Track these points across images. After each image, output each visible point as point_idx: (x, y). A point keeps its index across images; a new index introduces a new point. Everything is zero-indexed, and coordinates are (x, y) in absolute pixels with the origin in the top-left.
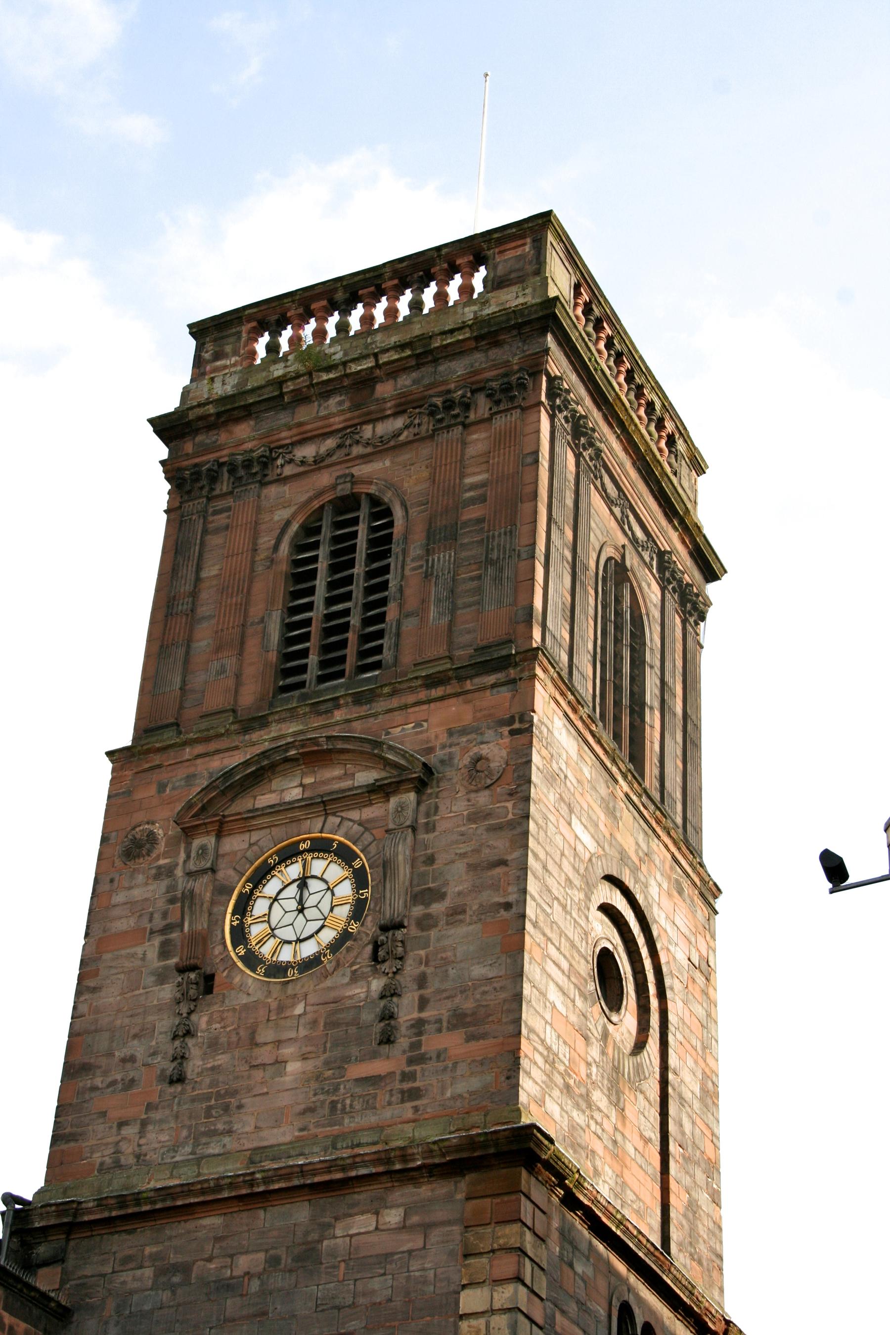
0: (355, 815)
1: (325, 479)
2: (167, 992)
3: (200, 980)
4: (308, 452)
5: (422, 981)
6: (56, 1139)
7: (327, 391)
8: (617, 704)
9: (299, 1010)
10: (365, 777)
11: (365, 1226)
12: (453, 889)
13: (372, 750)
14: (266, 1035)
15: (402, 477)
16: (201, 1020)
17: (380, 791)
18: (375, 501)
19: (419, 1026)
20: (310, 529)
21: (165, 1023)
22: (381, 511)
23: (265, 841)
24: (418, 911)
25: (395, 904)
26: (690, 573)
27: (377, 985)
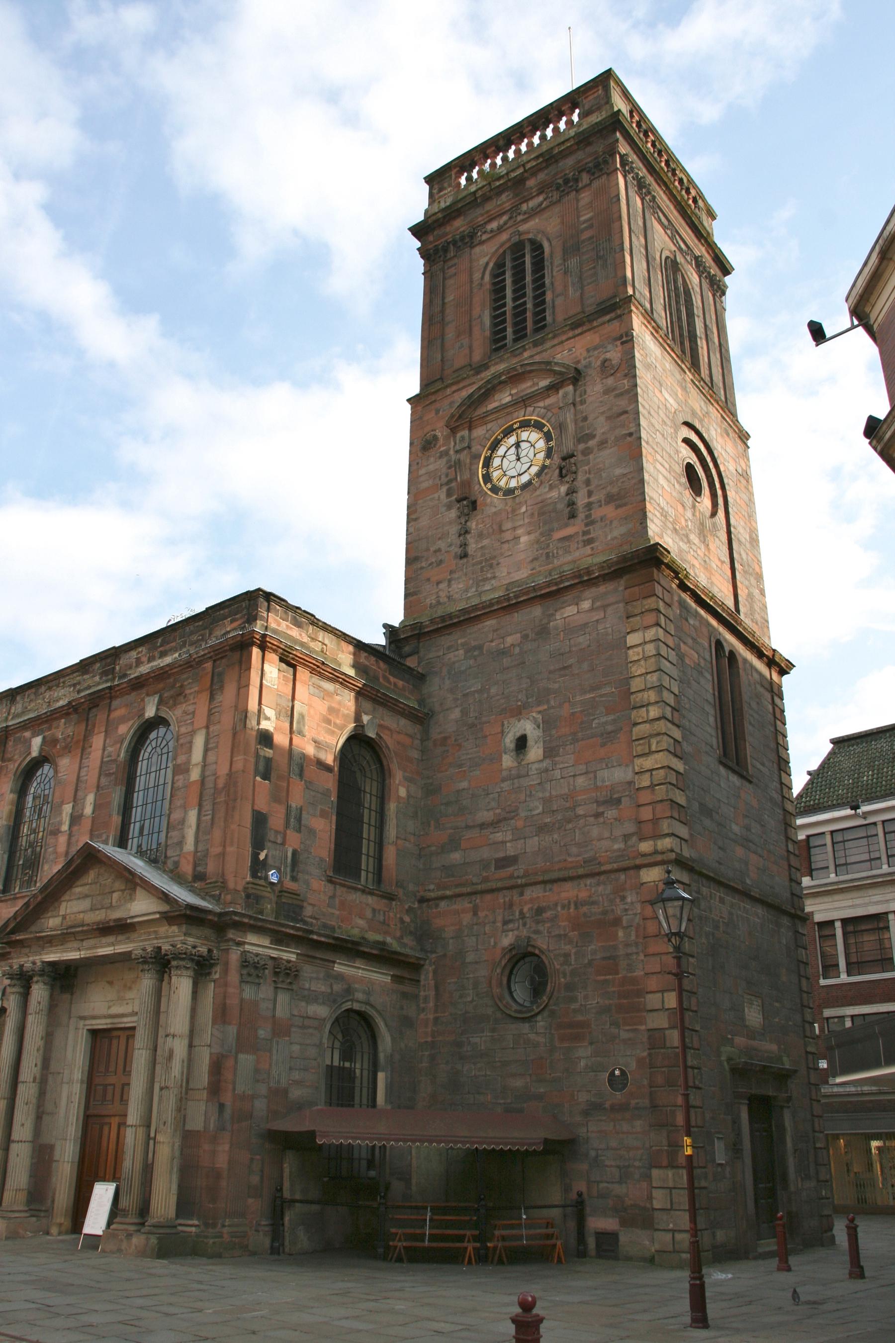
0: (541, 404)
1: (504, 237)
2: (453, 514)
3: (469, 504)
4: (494, 225)
5: (588, 482)
6: (407, 595)
7: (499, 191)
8: (681, 335)
9: (523, 509)
10: (544, 383)
11: (570, 612)
12: (599, 431)
13: (546, 367)
14: (507, 525)
15: (545, 226)
16: (472, 525)
17: (553, 388)
18: (532, 242)
19: (589, 506)
20: (500, 266)
21: (454, 529)
22: (537, 247)
23: (495, 428)
24: (581, 446)
25: (569, 445)
26: (714, 270)
27: (563, 489)
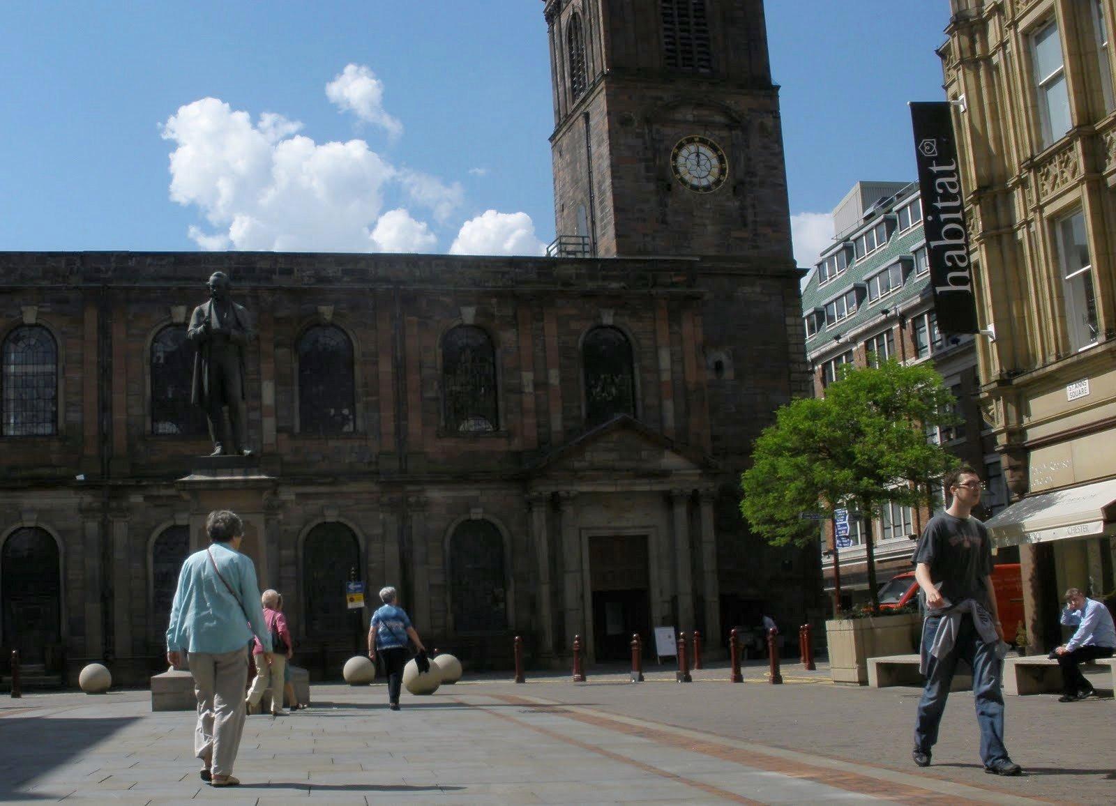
0: (717, 133)
5: (754, 206)
9: (708, 206)
17: (730, 127)
19: (755, 222)
27: (737, 204)
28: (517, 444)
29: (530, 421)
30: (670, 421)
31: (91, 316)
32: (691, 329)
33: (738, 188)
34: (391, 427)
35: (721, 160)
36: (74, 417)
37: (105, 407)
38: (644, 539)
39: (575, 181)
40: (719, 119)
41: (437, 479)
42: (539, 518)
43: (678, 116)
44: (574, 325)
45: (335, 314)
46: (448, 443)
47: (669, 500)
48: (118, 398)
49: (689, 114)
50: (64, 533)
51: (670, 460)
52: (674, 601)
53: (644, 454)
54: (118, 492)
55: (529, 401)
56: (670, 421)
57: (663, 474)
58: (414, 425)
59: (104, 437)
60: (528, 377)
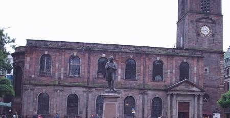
11: (213, 56)
13: (212, 20)
17: (212, 23)
25: (213, 33)
28: (166, 84)
29: (169, 79)
30: (195, 81)
31: (87, 55)
32: (201, 63)
33: (213, 35)
34: (142, 79)
35: (210, 29)
36: (83, 74)
37: (89, 72)
38: (189, 103)
39: (181, 32)
40: (210, 21)
41: (150, 90)
42: (169, 98)
43: (202, 21)
44: (178, 62)
45: (133, 57)
46: (153, 83)
47: (194, 96)
48: (91, 71)
49: (204, 20)
50: (79, 95)
51: (195, 89)
52: (194, 115)
53: (190, 87)
54: (90, 88)
55: (169, 76)
56: (195, 81)
57: (194, 91)
58: (147, 79)
59: (88, 78)
60: (169, 71)
